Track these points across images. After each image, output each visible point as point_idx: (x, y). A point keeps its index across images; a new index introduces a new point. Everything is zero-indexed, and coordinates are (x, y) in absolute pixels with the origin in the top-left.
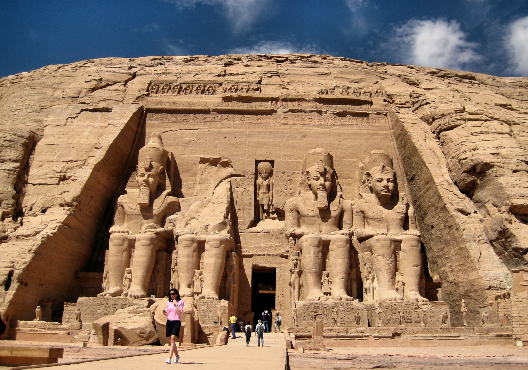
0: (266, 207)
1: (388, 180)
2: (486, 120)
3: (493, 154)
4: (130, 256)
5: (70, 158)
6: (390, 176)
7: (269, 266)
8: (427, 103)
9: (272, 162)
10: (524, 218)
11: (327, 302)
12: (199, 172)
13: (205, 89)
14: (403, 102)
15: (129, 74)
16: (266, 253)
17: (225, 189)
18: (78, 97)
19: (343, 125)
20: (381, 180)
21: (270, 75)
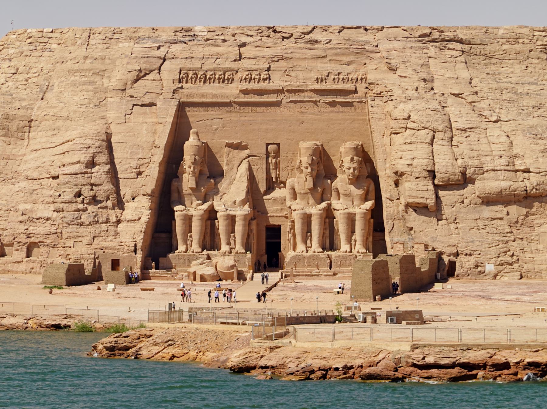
0: (274, 180)
1: (354, 169)
2: (419, 130)
3: (408, 165)
4: (190, 226)
5: (140, 156)
6: (355, 165)
7: (276, 223)
8: (392, 100)
9: (278, 145)
10: (415, 208)
11: (306, 254)
12: (225, 154)
13: (226, 78)
14: (379, 92)
15: (160, 58)
16: (275, 215)
17: (245, 170)
18: (125, 89)
19: (332, 112)
20: (349, 169)
21: (276, 59)
